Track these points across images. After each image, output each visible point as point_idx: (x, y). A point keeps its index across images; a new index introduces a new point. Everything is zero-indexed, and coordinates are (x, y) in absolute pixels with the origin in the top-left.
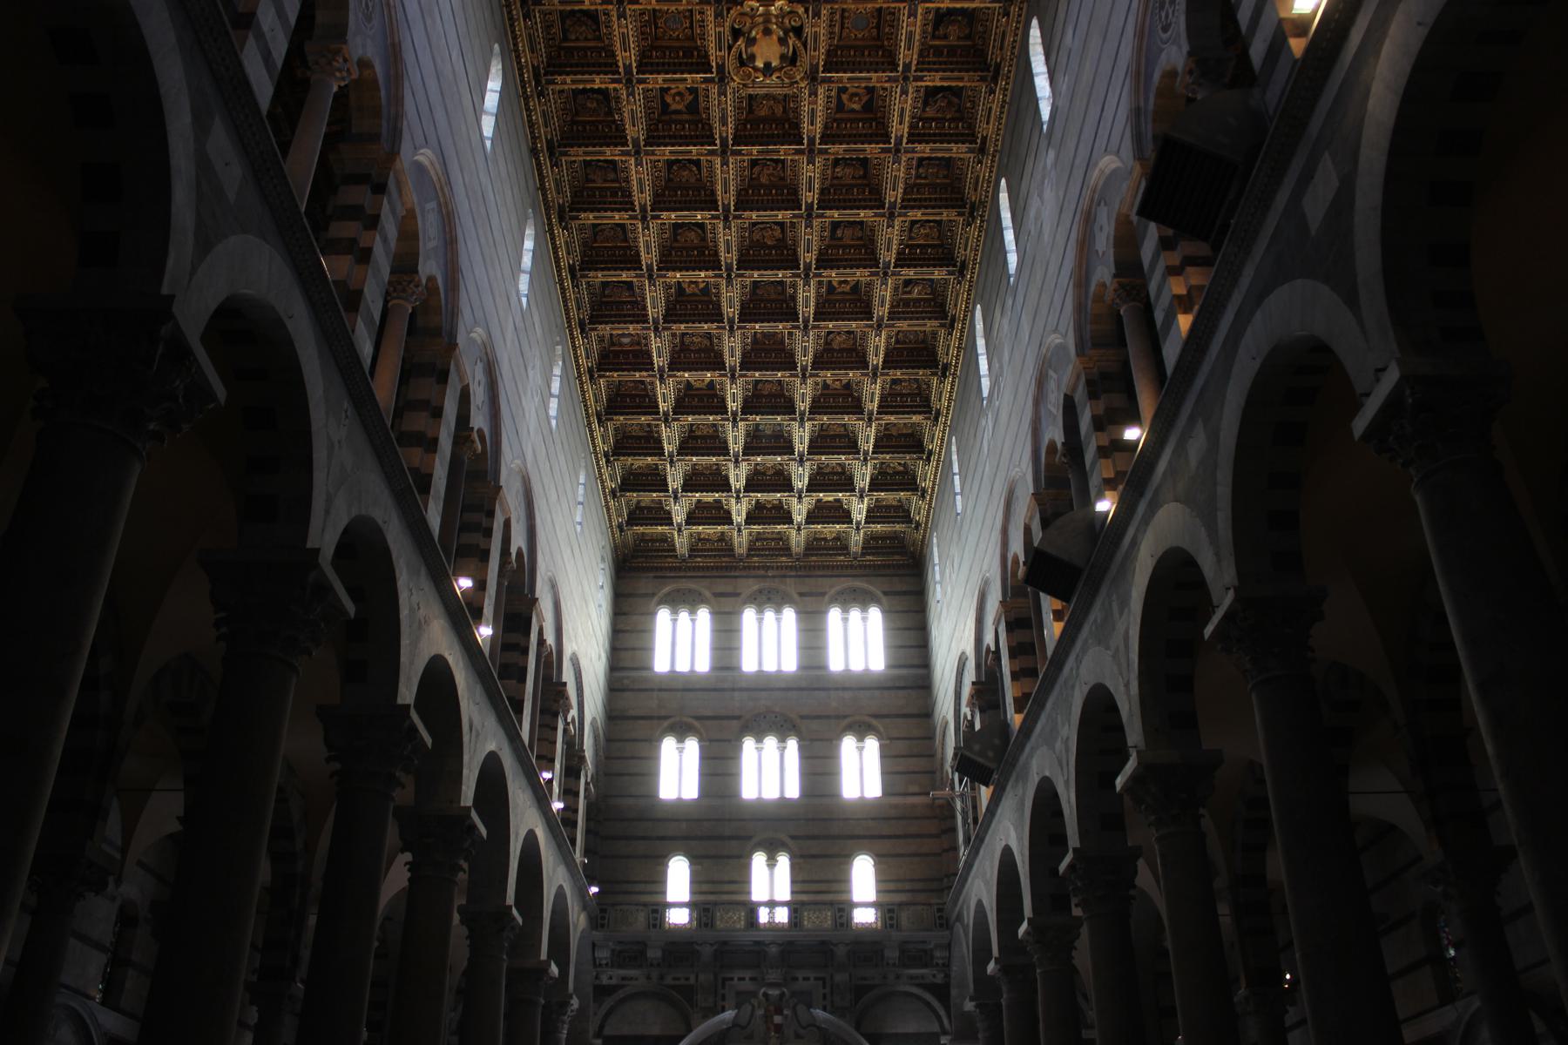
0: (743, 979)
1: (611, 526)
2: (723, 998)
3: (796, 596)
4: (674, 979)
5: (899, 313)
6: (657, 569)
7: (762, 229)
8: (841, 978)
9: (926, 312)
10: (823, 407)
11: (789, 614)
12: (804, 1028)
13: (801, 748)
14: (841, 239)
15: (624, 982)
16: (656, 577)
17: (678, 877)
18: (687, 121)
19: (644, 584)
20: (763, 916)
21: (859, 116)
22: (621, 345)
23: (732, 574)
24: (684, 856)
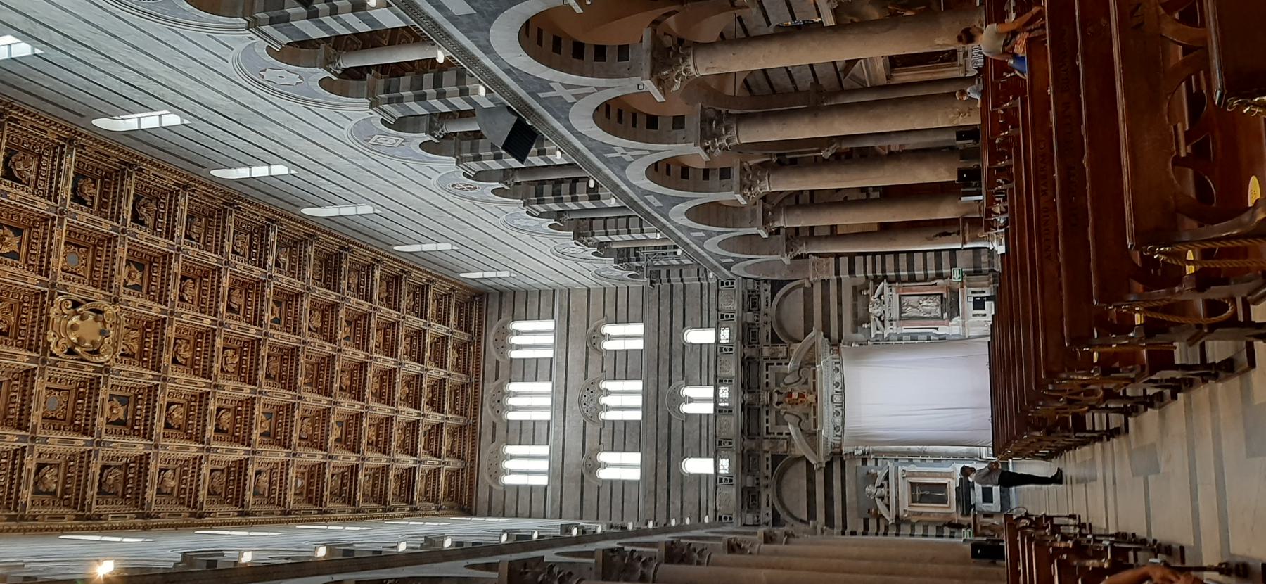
1: (438, 515)
4: (767, 468)
7: (226, 364)
8: (766, 352)
10: (363, 342)
12: (801, 378)
14: (239, 306)
17: (698, 466)
18: (135, 406)
21: (147, 275)
22: (302, 487)
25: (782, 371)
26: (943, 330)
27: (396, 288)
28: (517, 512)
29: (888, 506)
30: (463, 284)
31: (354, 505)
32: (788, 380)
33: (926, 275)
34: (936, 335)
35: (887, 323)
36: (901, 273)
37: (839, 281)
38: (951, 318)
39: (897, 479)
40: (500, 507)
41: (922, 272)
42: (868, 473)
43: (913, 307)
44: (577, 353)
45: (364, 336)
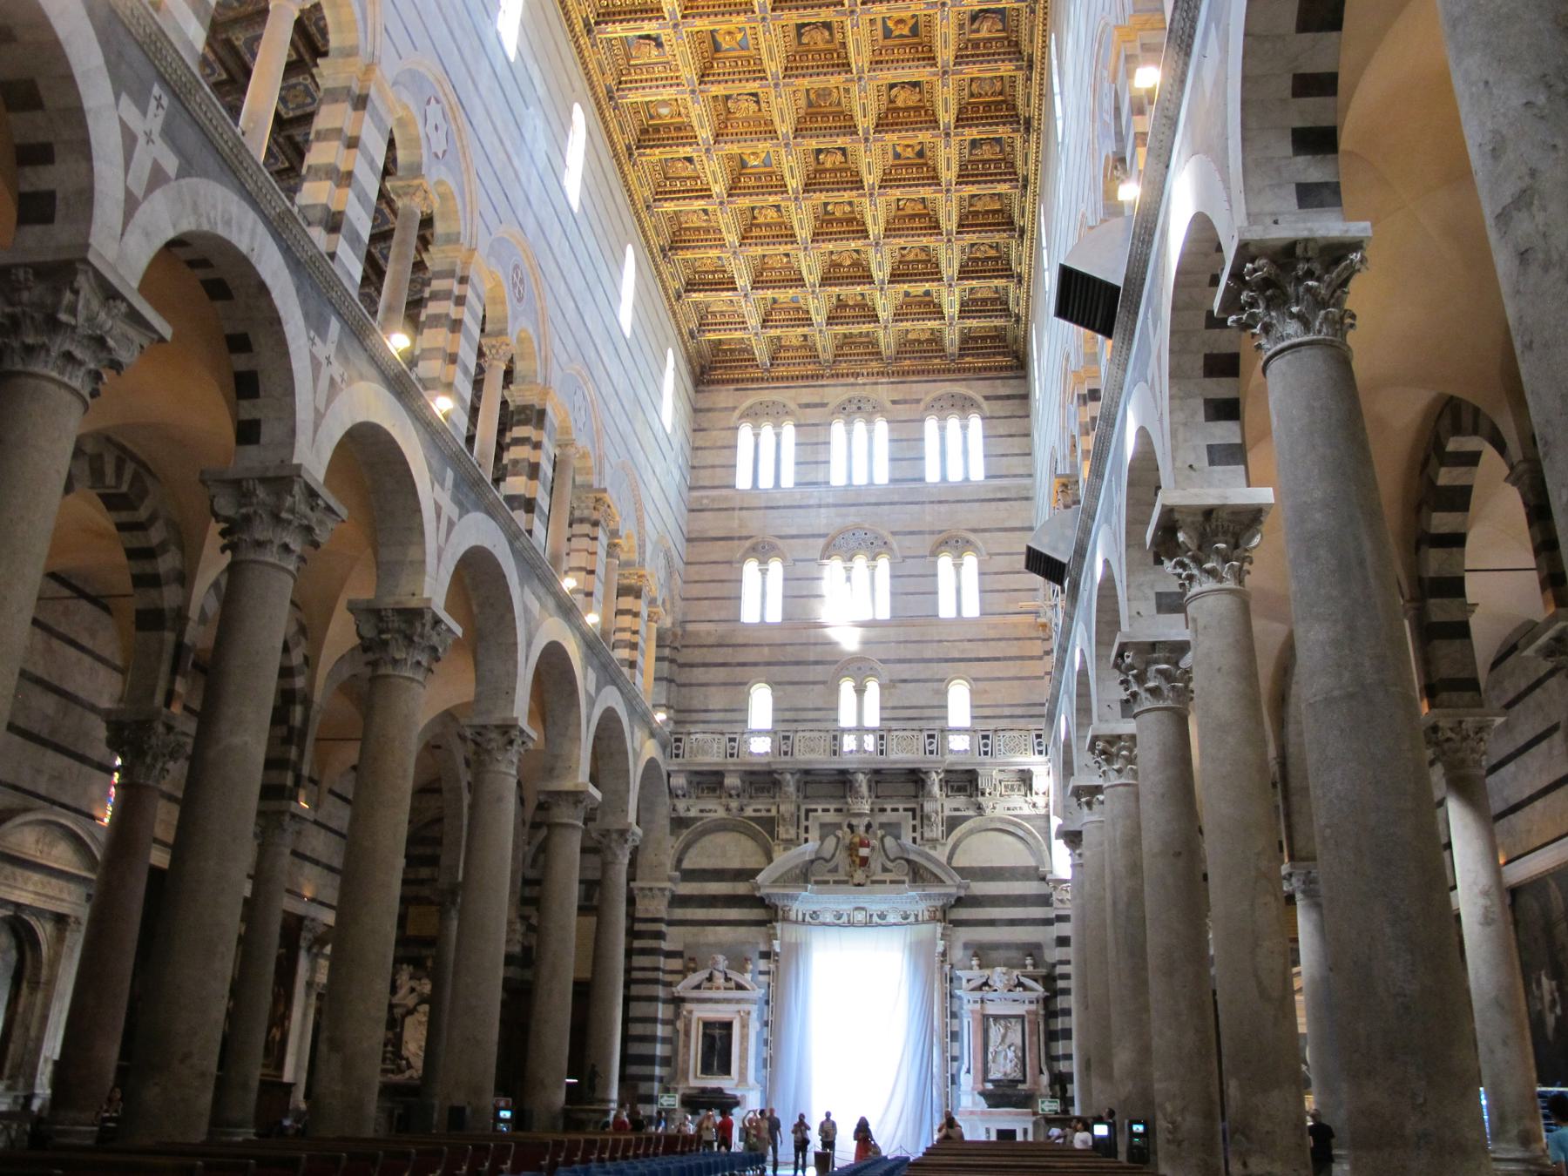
0: (828, 810)
2: (807, 830)
3: (889, 405)
4: (755, 811)
5: (967, 56)
6: (737, 381)
9: (999, 54)
10: (895, 180)
11: (881, 427)
12: (892, 861)
13: (893, 566)
15: (705, 815)
16: (737, 390)
17: (761, 705)
19: (723, 396)
20: (849, 743)
22: (660, 117)
23: (820, 383)
24: (767, 683)
25: (903, 832)
26: (967, 1081)
27: (994, 225)
28: (697, 449)
29: (698, 987)
30: (1026, 340)
31: (655, 200)
32: (889, 841)
33: (1057, 1058)
34: (959, 1070)
35: (978, 995)
36: (1060, 1019)
37: (1048, 922)
38: (983, 1094)
39: (738, 1001)
40: (705, 425)
41: (1061, 1053)
42: (746, 960)
43: (1004, 1037)
44: (930, 517)
45: (904, 179)
